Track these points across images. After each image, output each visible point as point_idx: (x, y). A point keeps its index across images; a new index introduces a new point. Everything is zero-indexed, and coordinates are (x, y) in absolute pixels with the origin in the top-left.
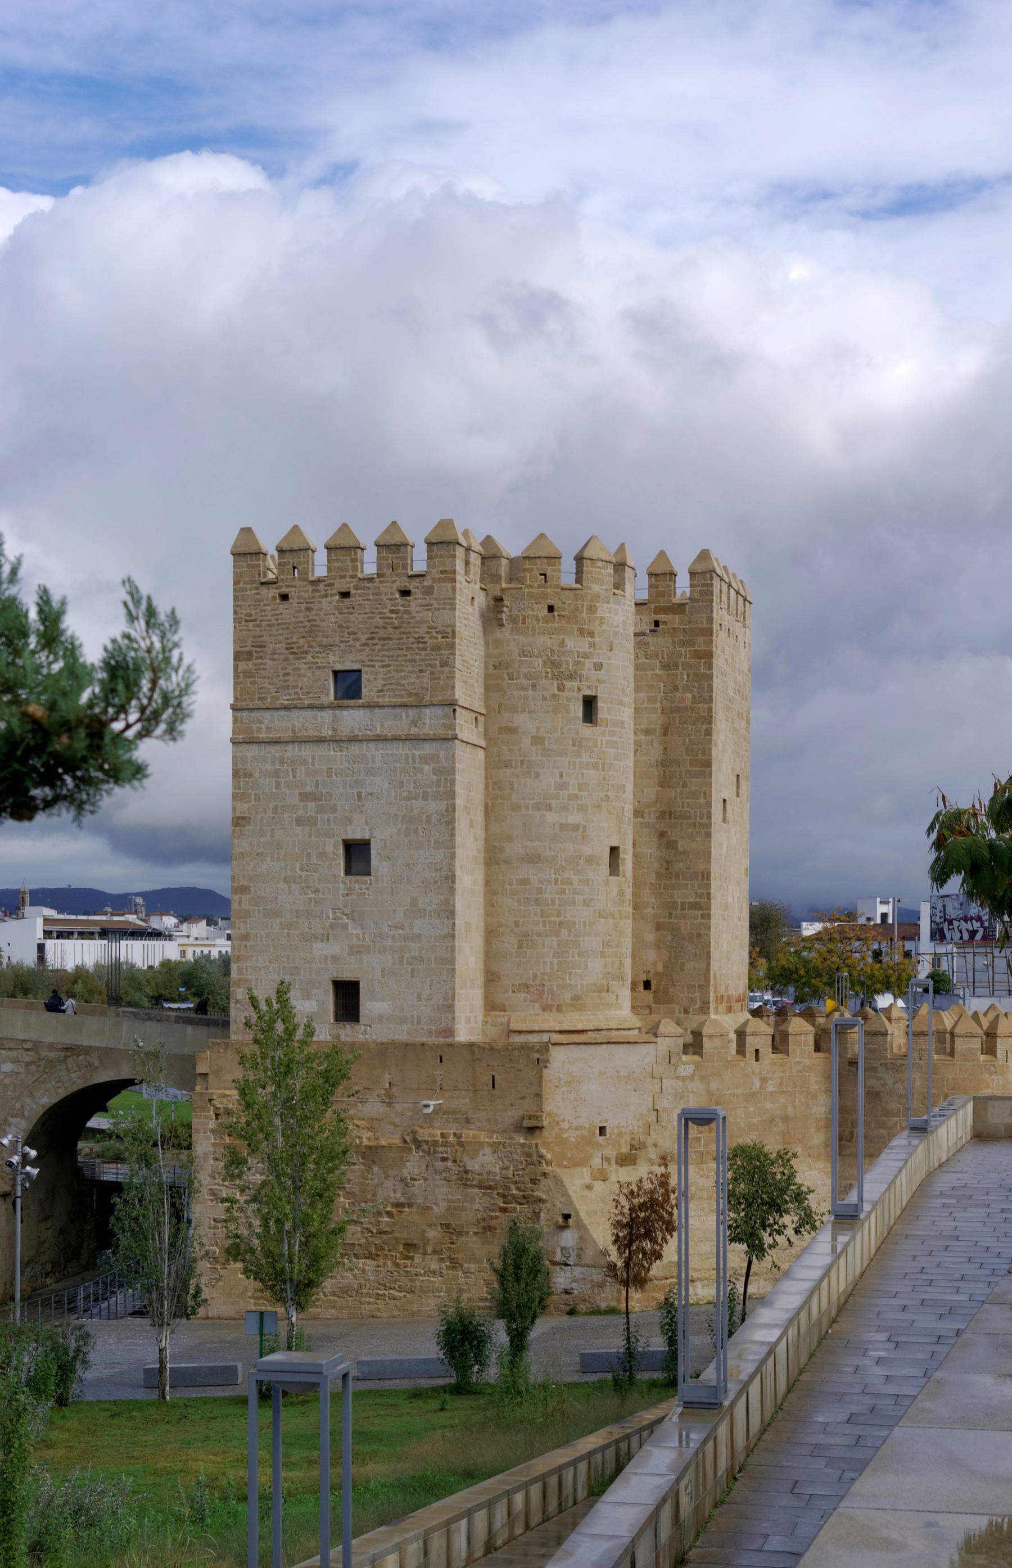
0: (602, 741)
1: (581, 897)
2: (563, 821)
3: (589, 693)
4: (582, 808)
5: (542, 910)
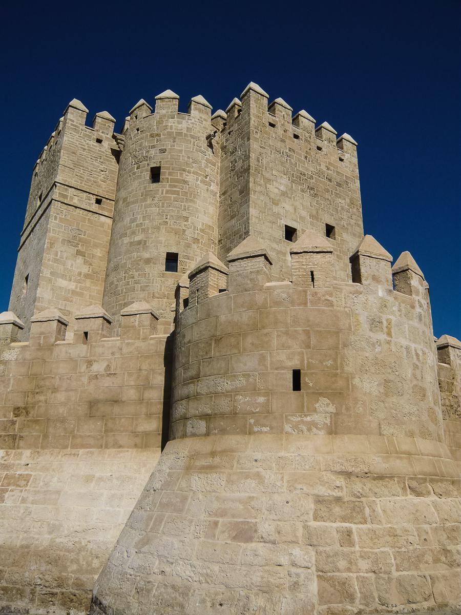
0: (163, 191)
1: (140, 285)
2: (132, 241)
3: (155, 165)
4: (143, 230)
5: (116, 298)
